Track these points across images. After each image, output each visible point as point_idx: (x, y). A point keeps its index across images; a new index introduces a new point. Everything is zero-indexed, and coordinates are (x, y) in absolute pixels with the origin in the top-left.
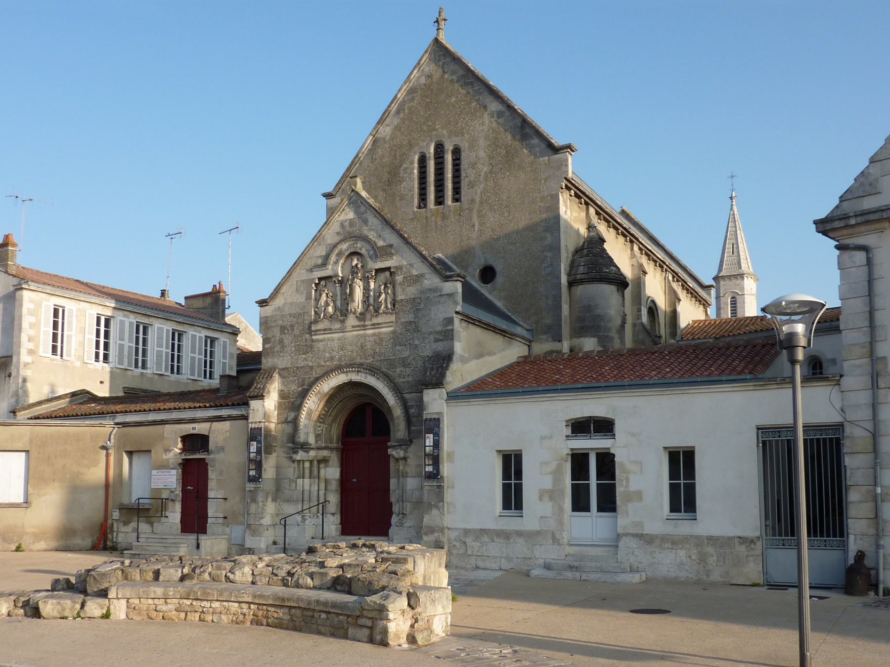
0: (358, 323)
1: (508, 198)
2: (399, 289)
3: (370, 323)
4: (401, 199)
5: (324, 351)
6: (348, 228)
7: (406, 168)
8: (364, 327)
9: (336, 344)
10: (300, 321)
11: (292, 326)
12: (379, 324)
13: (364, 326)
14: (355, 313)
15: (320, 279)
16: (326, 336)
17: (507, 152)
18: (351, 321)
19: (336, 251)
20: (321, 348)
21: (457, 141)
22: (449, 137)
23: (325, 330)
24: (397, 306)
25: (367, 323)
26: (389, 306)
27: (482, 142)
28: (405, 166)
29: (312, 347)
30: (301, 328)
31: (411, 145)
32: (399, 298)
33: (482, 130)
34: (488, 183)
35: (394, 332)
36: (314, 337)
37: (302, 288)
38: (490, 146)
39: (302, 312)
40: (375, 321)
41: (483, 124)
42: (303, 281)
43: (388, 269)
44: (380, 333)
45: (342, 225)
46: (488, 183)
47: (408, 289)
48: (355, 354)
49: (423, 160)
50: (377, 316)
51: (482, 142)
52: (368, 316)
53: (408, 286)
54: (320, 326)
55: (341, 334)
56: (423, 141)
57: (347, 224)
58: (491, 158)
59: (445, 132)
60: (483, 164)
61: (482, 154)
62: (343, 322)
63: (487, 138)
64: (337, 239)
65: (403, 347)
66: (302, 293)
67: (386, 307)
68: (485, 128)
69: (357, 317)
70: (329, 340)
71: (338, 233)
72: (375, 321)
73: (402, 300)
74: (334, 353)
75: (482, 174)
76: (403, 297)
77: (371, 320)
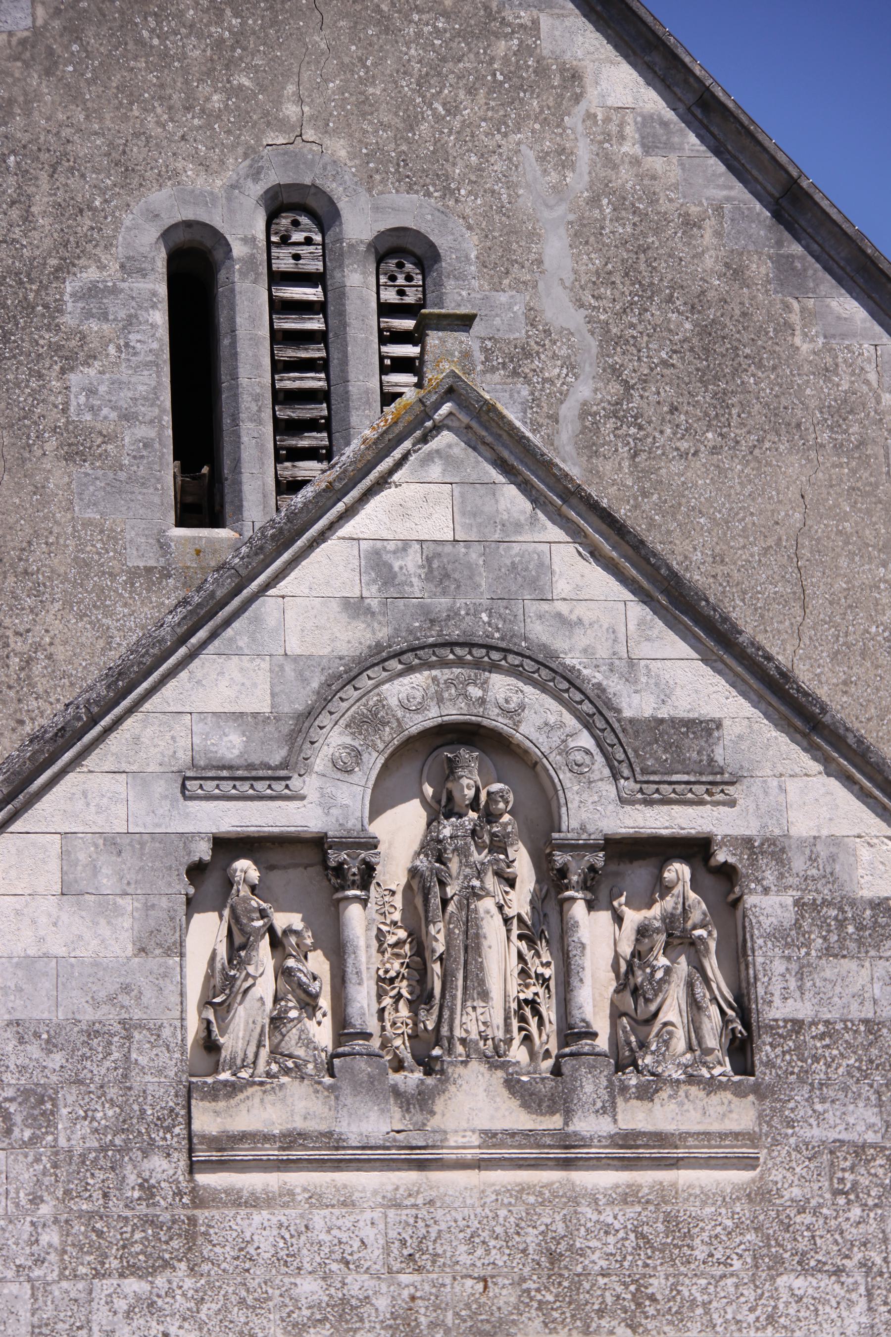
0: (524, 1121)
1: (719, 559)
2: (771, 967)
3: (603, 1126)
4: (74, 453)
5: (286, 1260)
6: (417, 587)
7: (92, 292)
8: (568, 1154)
9: (371, 1230)
10: (99, 1070)
11: (39, 1102)
12: (660, 1139)
13: (566, 1140)
14: (495, 1059)
15: (228, 846)
16: (297, 1179)
17: (704, 331)
18: (475, 1105)
19: (349, 704)
20: (265, 1244)
21: (409, 210)
22: (369, 183)
23: (291, 1139)
24: (765, 1051)
25: (589, 1124)
26: (711, 1042)
27: (556, 249)
28: (92, 274)
29: (191, 1233)
30: (106, 1114)
31: (129, 175)
32: (779, 1004)
33: (558, 190)
34: (607, 467)
35: (760, 1195)
36: (202, 1179)
37: (107, 882)
38: (603, 277)
39: (110, 1015)
40: (636, 1117)
41: (563, 158)
42: (112, 843)
43: (695, 849)
44: (664, 1195)
45: (378, 564)
46: (607, 467)
47: (830, 969)
48: (505, 1296)
49: (194, 271)
50: (646, 1094)
51: (556, 249)
52: (591, 1085)
53: (828, 952)
54: (255, 1114)
55: (411, 1177)
56: (204, 165)
57: (412, 562)
58: (610, 341)
59: (339, 148)
60: (572, 367)
61: (562, 312)
62: (420, 1102)
63: (583, 233)
64: (350, 638)
65: (826, 1282)
66: (107, 910)
67: (695, 1044)
68: (578, 181)
69: (512, 1085)
70: (316, 1199)
71: (355, 607)
72: (636, 1117)
73: (798, 1025)
74: (357, 1284)
75: (569, 410)
76: (803, 1010)
77: (609, 1109)
